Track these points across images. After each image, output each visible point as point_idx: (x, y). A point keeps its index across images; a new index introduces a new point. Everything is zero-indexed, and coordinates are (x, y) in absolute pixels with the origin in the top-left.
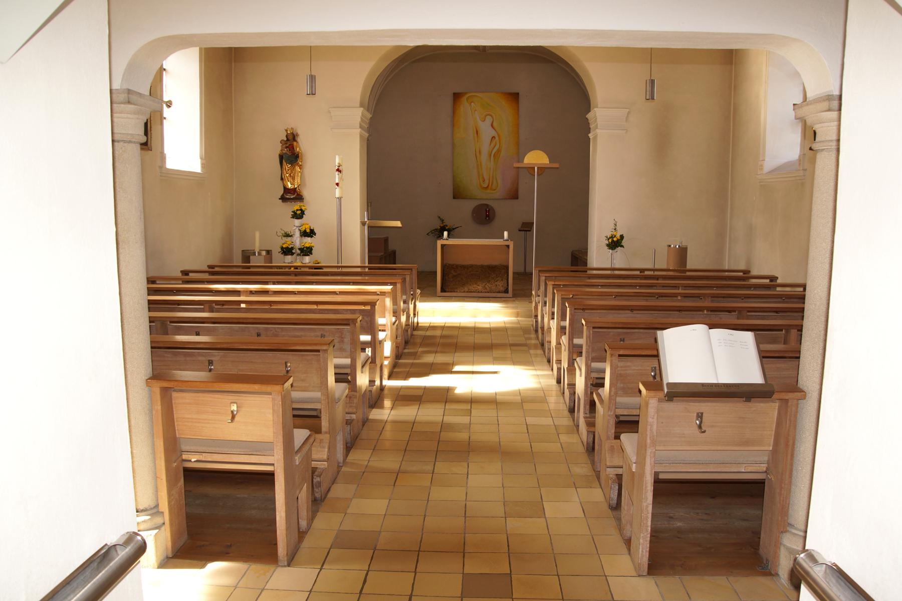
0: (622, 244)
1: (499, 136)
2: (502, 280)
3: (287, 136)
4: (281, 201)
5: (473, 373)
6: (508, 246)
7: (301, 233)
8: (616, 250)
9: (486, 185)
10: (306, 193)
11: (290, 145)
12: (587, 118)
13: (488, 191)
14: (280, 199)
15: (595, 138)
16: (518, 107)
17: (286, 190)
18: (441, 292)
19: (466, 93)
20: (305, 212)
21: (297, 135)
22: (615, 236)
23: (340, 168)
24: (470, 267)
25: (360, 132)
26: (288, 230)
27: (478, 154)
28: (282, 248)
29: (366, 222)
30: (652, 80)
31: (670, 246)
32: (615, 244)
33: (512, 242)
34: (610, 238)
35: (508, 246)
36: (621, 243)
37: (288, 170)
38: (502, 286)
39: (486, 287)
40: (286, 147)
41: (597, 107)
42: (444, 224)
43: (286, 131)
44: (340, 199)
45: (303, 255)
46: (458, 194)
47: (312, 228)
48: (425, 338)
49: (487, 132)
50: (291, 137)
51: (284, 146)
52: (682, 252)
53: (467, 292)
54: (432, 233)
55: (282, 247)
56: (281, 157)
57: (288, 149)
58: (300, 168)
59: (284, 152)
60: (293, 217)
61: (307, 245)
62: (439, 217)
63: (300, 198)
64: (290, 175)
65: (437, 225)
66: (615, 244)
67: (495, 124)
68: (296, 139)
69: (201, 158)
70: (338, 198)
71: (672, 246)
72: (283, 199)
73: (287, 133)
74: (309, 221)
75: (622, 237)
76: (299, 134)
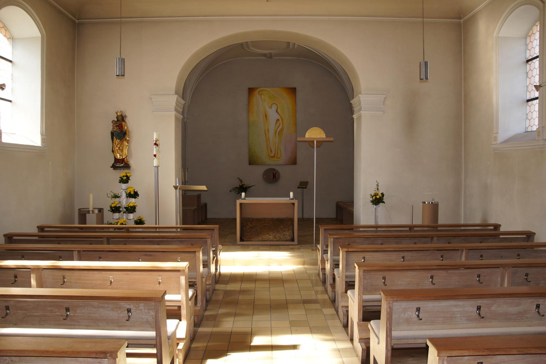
0: (384, 201)
1: (282, 118)
2: (289, 230)
3: (117, 118)
4: (112, 168)
5: (272, 348)
6: (293, 204)
7: (127, 195)
8: (379, 205)
9: (273, 155)
10: (132, 163)
11: (119, 124)
12: (351, 103)
13: (275, 159)
14: (111, 167)
15: (359, 118)
16: (296, 98)
17: (117, 160)
18: (240, 241)
19: (257, 88)
20: (130, 178)
21: (126, 116)
22: (378, 195)
23: (158, 143)
24: (263, 220)
25: (175, 114)
26: (116, 192)
27: (267, 132)
28: (111, 207)
29: (178, 186)
30: (425, 62)
31: (424, 203)
32: (377, 200)
33: (297, 201)
34: (374, 196)
35: (293, 204)
36: (383, 199)
37: (118, 144)
38: (289, 235)
39: (276, 236)
40: (116, 126)
41: (361, 94)
42: (243, 184)
43: (117, 113)
44: (157, 167)
45: (128, 213)
46: (252, 162)
47: (136, 191)
48: (227, 293)
49: (273, 116)
50: (120, 118)
51: (115, 125)
52: (435, 207)
53: (261, 241)
54: (234, 190)
55: (111, 206)
56: (112, 134)
57: (118, 127)
58: (128, 143)
59: (114, 130)
60: (120, 182)
61: (131, 205)
62: (239, 179)
63: (127, 166)
64: (119, 148)
65: (237, 184)
66: (377, 200)
67: (279, 111)
68: (124, 119)
69: (42, 135)
70: (156, 167)
71: (426, 202)
72: (114, 167)
73: (117, 115)
74: (133, 185)
75: (383, 194)
76: (126, 115)
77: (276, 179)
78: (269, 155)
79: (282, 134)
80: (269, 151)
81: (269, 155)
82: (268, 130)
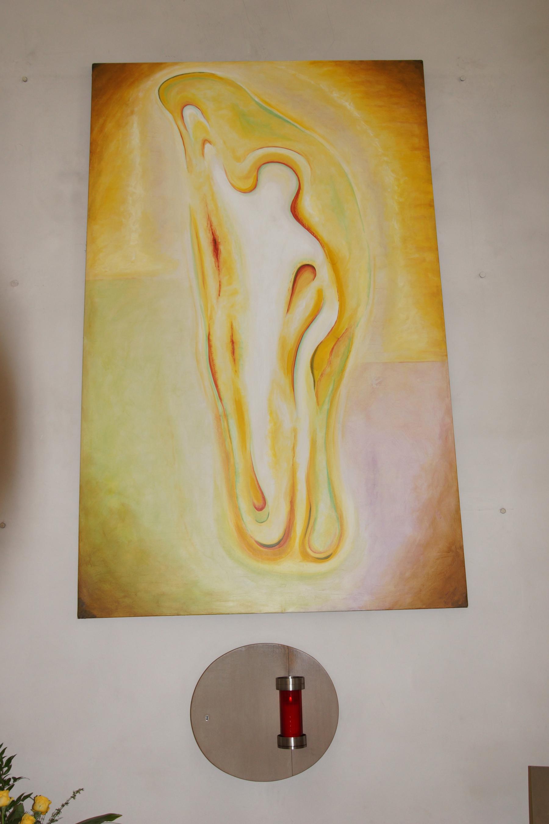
16: (425, 124)
19: (155, 67)
77: (300, 745)
78: (241, 532)
79: (343, 370)
80: (244, 505)
81: (241, 532)
82: (233, 342)
